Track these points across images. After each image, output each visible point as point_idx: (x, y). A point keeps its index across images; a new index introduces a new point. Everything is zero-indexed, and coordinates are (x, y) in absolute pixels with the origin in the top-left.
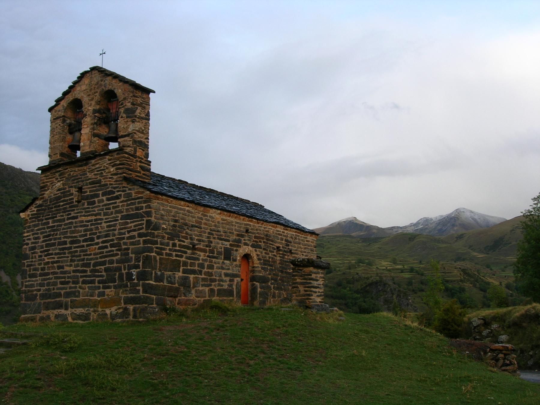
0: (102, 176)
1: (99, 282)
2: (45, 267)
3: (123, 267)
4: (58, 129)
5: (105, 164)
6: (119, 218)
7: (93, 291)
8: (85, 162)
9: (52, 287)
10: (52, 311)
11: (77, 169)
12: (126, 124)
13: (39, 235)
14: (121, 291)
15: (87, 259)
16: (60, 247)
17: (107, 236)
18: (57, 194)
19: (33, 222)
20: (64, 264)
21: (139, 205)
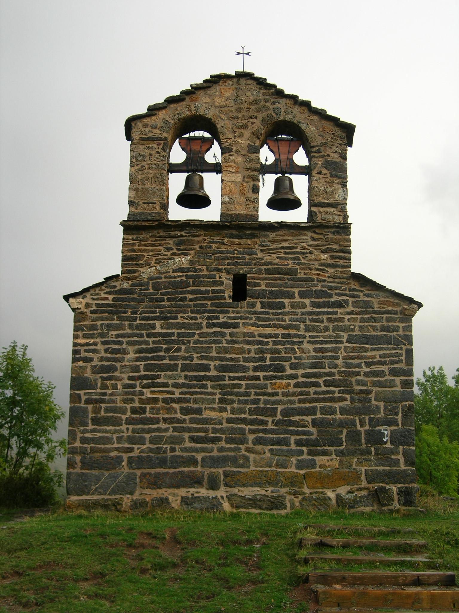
0: (298, 264)
1: (299, 443)
2: (146, 408)
3: (358, 421)
4: (152, 158)
5: (304, 244)
6: (345, 340)
7: (287, 458)
8: (249, 232)
9: (168, 447)
10: (171, 491)
11: (226, 240)
12: (331, 186)
13: (124, 346)
14: (356, 460)
15: (266, 402)
16: (191, 374)
17: (313, 366)
18: (171, 277)
19: (102, 319)
20: (203, 407)
21: (390, 324)
